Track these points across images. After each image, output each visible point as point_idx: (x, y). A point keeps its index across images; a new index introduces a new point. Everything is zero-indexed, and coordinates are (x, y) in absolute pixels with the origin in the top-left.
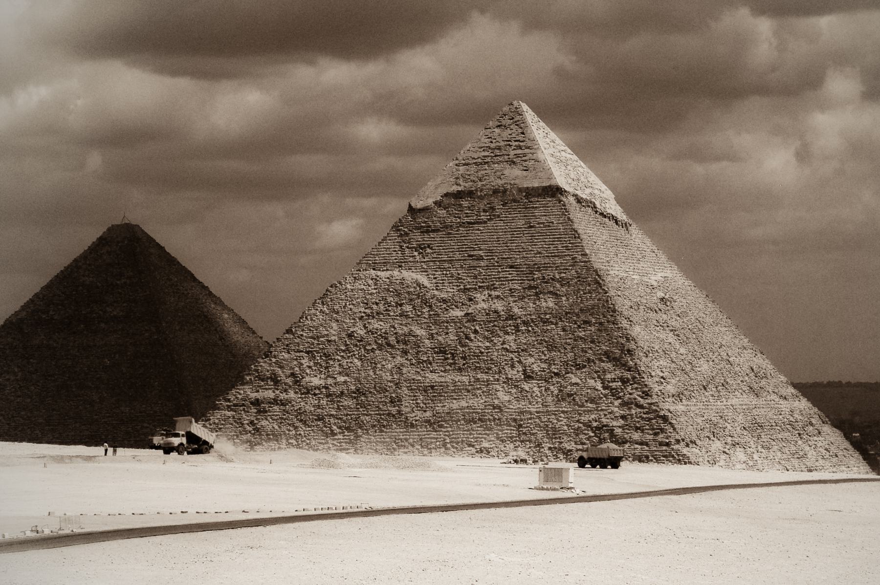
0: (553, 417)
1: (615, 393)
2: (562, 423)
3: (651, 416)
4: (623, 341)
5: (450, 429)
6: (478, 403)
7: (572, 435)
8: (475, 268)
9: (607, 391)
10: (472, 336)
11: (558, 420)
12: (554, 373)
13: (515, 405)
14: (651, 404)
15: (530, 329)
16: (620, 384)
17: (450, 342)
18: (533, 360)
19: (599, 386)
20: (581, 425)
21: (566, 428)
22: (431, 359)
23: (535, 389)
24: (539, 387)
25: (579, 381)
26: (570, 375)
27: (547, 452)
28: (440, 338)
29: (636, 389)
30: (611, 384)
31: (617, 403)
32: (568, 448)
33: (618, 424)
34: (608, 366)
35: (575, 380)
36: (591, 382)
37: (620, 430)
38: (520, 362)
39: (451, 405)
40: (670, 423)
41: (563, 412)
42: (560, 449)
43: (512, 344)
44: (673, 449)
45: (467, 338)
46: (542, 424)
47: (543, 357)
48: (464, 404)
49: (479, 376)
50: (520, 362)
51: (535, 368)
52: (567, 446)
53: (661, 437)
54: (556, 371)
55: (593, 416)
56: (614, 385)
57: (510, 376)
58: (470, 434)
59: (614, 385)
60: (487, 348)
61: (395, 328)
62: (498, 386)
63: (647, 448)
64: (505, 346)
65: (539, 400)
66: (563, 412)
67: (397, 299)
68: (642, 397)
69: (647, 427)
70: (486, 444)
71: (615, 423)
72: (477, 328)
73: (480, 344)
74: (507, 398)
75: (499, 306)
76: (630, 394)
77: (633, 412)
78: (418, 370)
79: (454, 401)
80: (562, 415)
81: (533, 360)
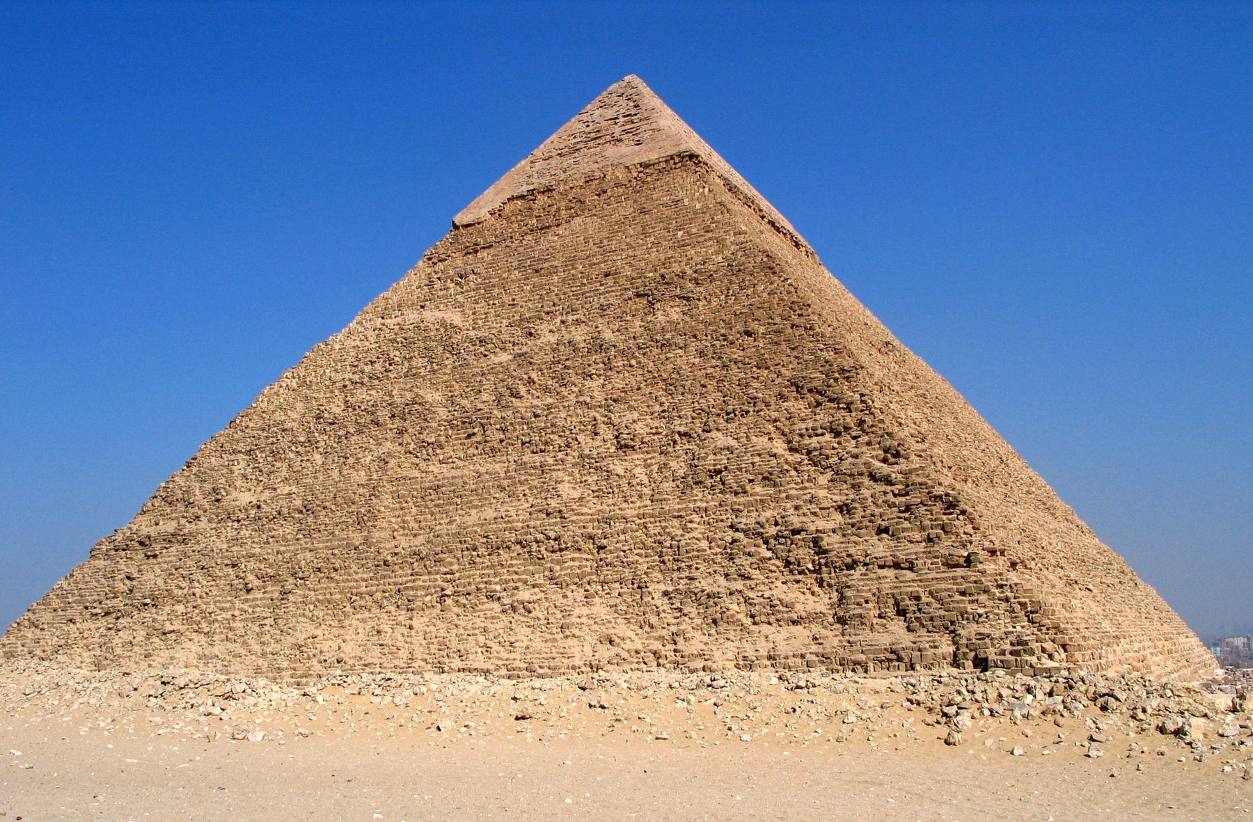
0: (675, 522)
1: (816, 459)
2: (696, 534)
3: (914, 498)
4: (830, 355)
5: (455, 567)
6: (518, 511)
7: (719, 558)
8: (541, 286)
9: (797, 457)
10: (522, 390)
11: (684, 528)
12: (679, 433)
13: (592, 507)
14: (910, 472)
15: (633, 362)
16: (828, 437)
17: (480, 406)
18: (636, 415)
19: (779, 446)
20: (740, 535)
21: (704, 544)
22: (443, 439)
23: (638, 471)
24: (647, 466)
25: (733, 443)
26: (714, 434)
27: (659, 603)
28: (464, 402)
29: (869, 444)
30: (807, 441)
31: (823, 480)
32: (709, 589)
33: (831, 525)
34: (798, 406)
35: (721, 440)
36: (762, 442)
37: (836, 538)
38: (610, 423)
39: (467, 518)
40: (963, 512)
41: (697, 511)
42: (690, 593)
43: (595, 394)
44: (983, 573)
45: (517, 395)
46: (649, 541)
47: (657, 408)
48: (490, 514)
49: (525, 459)
50: (610, 423)
51: (640, 428)
52: (705, 584)
53: (945, 546)
54: (682, 429)
55: (768, 514)
56: (814, 442)
57: (587, 452)
58: (496, 575)
59: (814, 442)
60: (549, 407)
61: (391, 396)
62: (560, 474)
63: (909, 575)
64: (581, 399)
65: (647, 491)
66: (697, 511)
67: (404, 352)
68: (885, 461)
69: (906, 525)
70: (525, 595)
71: (821, 524)
72: (534, 376)
73: (535, 402)
74: (577, 494)
75: (579, 335)
76: (856, 456)
77: (866, 493)
78: (417, 461)
79: (474, 512)
80: (696, 518)
81: (636, 415)
